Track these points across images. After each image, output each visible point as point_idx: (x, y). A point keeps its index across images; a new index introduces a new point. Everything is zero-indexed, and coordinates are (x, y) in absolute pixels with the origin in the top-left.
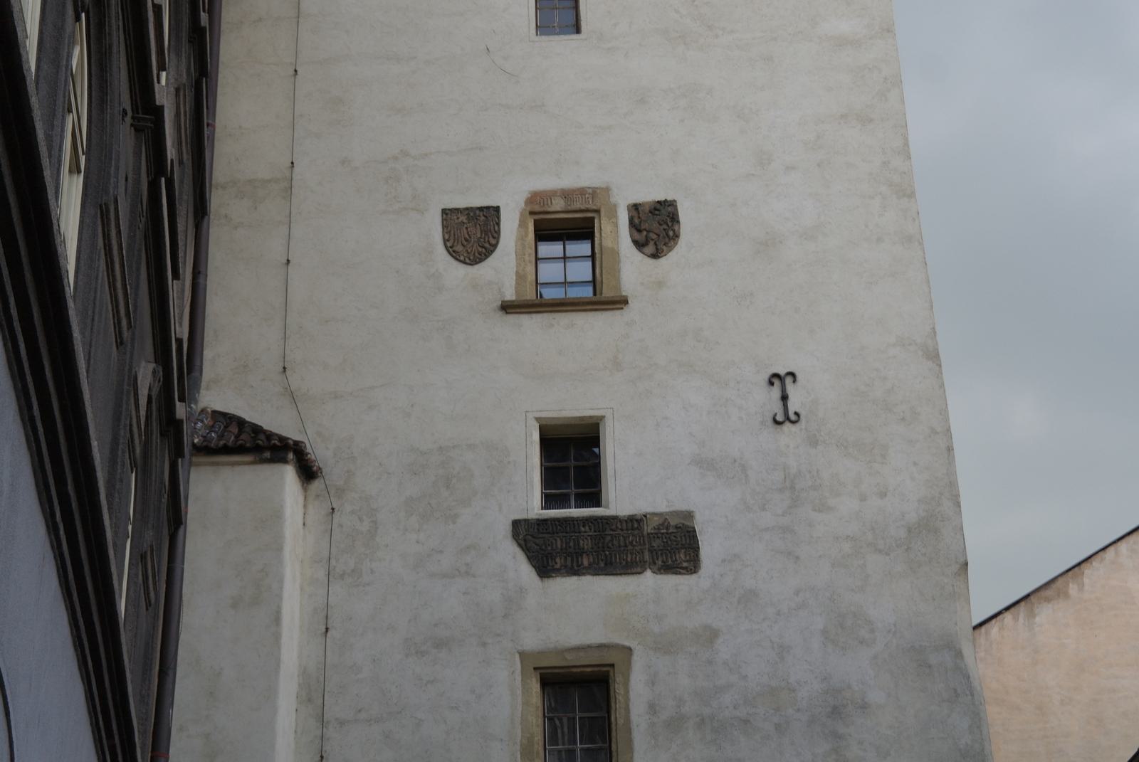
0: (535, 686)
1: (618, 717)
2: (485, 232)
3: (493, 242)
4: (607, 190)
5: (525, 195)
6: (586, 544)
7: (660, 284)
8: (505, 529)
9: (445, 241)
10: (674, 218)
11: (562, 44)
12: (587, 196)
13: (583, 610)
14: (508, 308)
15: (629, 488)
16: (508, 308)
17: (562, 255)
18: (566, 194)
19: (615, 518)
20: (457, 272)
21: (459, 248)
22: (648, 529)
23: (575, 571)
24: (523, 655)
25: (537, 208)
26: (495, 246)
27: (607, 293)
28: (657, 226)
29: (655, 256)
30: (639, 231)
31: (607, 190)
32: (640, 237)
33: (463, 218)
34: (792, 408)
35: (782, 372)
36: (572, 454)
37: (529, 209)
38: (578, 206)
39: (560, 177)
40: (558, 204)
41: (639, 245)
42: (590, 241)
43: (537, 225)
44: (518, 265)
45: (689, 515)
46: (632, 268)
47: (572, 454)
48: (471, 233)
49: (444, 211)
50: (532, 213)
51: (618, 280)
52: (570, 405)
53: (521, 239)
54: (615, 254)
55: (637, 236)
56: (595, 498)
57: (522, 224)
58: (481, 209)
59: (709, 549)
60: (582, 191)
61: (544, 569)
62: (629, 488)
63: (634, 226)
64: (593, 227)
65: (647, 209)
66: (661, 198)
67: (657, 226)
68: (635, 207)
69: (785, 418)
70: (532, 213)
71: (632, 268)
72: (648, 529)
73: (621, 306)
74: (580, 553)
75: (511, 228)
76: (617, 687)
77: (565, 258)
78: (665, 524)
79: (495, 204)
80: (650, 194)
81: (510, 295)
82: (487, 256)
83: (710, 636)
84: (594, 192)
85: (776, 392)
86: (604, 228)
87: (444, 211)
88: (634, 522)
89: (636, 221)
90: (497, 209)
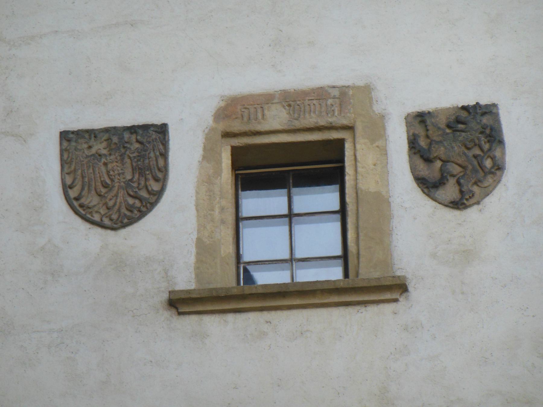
2: (141, 170)
3: (155, 186)
4: (367, 90)
5: (214, 104)
7: (467, 255)
9: (66, 188)
10: (494, 136)
12: (330, 101)
14: (180, 303)
16: (180, 303)
17: (285, 211)
18: (292, 100)
20: (89, 241)
21: (92, 200)
25: (237, 126)
26: (159, 194)
27: (367, 272)
29: (458, 204)
30: (428, 160)
31: (367, 90)
32: (432, 172)
33: (100, 147)
37: (222, 127)
38: (311, 120)
39: (279, 65)
40: (276, 118)
41: (428, 185)
42: (337, 187)
43: (237, 154)
44: (201, 227)
46: (416, 228)
48: (114, 171)
49: (65, 136)
50: (227, 135)
51: (388, 251)
53: (207, 181)
54: (382, 203)
55: (423, 169)
57: (209, 153)
58: (133, 129)
60: (320, 94)
63: (419, 151)
64: (341, 160)
65: (442, 121)
66: (470, 101)
67: (460, 151)
68: (421, 118)
70: (227, 135)
71: (416, 228)
73: (394, 296)
75: (187, 162)
77: (290, 216)
79: (157, 121)
80: (446, 95)
81: (185, 281)
82: (142, 214)
84: (343, 95)
86: (359, 159)
87: (65, 136)
89: (423, 143)
90: (162, 130)
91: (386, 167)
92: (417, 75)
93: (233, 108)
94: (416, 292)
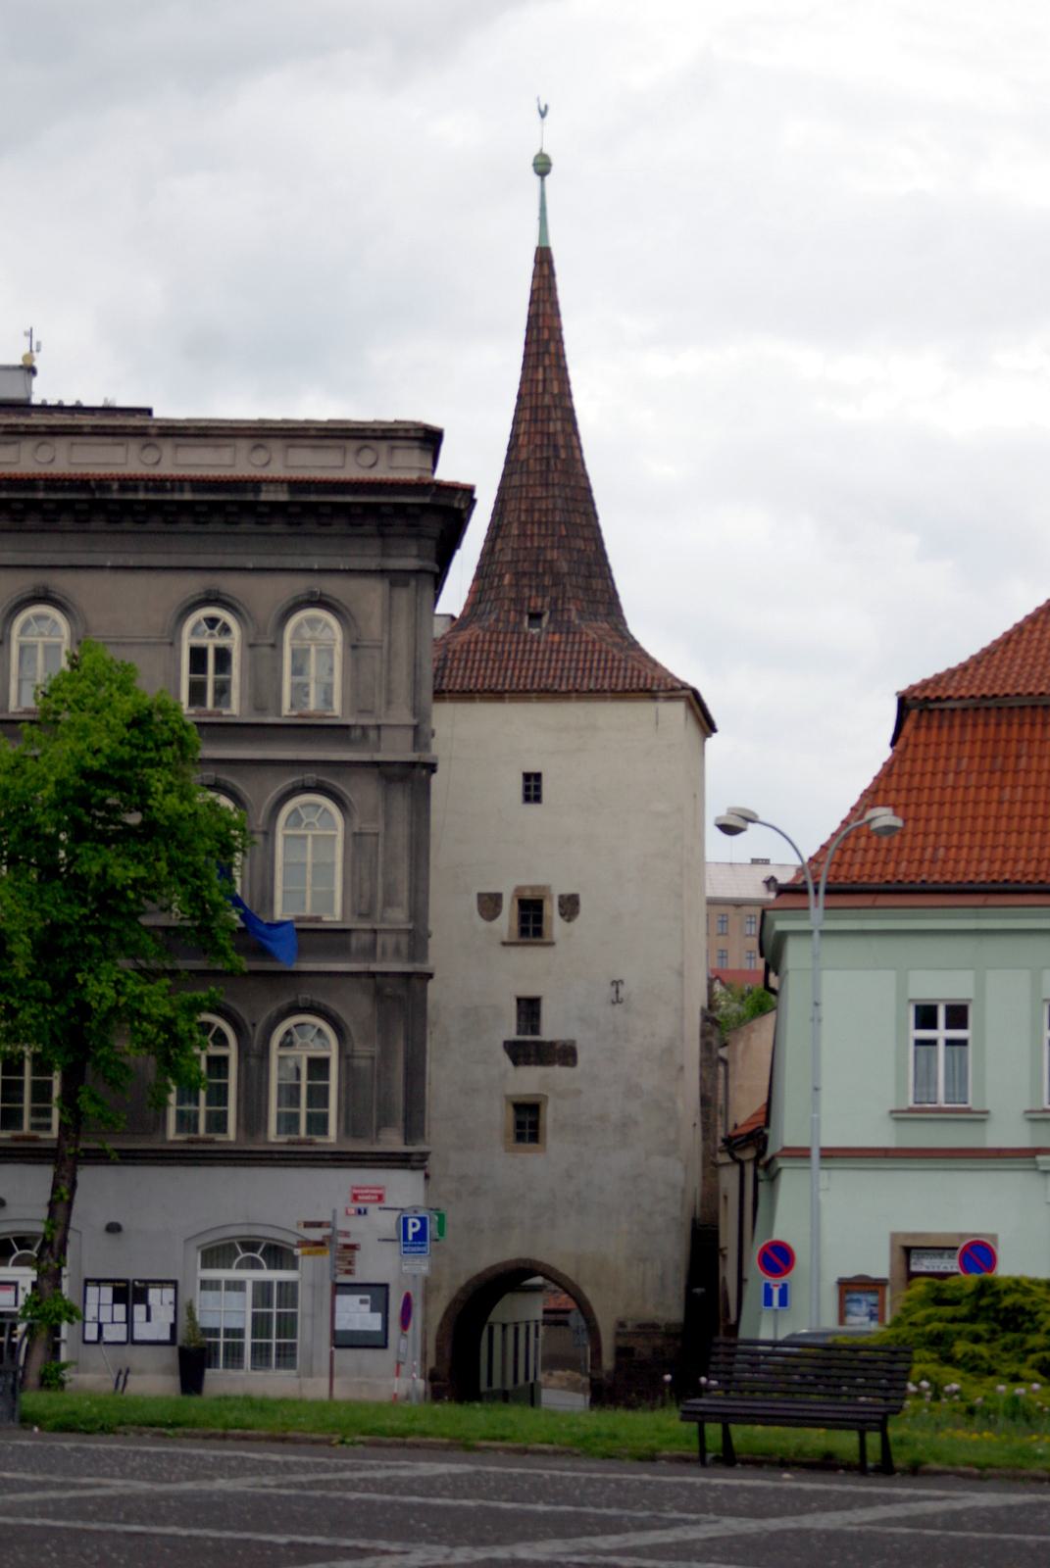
0: (511, 1111)
1: (541, 1123)
6: (532, 1052)
8: (500, 1044)
11: (533, 807)
13: (529, 1080)
14: (504, 944)
15: (551, 1030)
16: (504, 944)
18: (533, 888)
19: (542, 1043)
20: (482, 924)
22: (558, 1047)
23: (527, 1063)
24: (507, 1097)
27: (546, 939)
28: (570, 906)
29: (569, 921)
33: (486, 898)
34: (620, 996)
35: (616, 979)
36: (529, 1009)
38: (537, 893)
39: (530, 878)
41: (562, 915)
45: (574, 1042)
47: (529, 1009)
48: (490, 904)
52: (530, 992)
54: (551, 918)
56: (535, 1030)
57: (512, 902)
59: (581, 1056)
61: (516, 1063)
62: (551, 1030)
63: (561, 906)
67: (570, 906)
68: (561, 897)
69: (617, 1001)
72: (558, 1047)
74: (529, 1056)
76: (542, 1112)
78: (564, 1046)
80: (568, 890)
81: (506, 939)
83: (579, 1092)
84: (545, 888)
85: (614, 989)
86: (546, 906)
87: (480, 895)
88: (552, 1044)
91: (552, 910)
92: (560, 887)
93: (518, 889)
94: (558, 947)
